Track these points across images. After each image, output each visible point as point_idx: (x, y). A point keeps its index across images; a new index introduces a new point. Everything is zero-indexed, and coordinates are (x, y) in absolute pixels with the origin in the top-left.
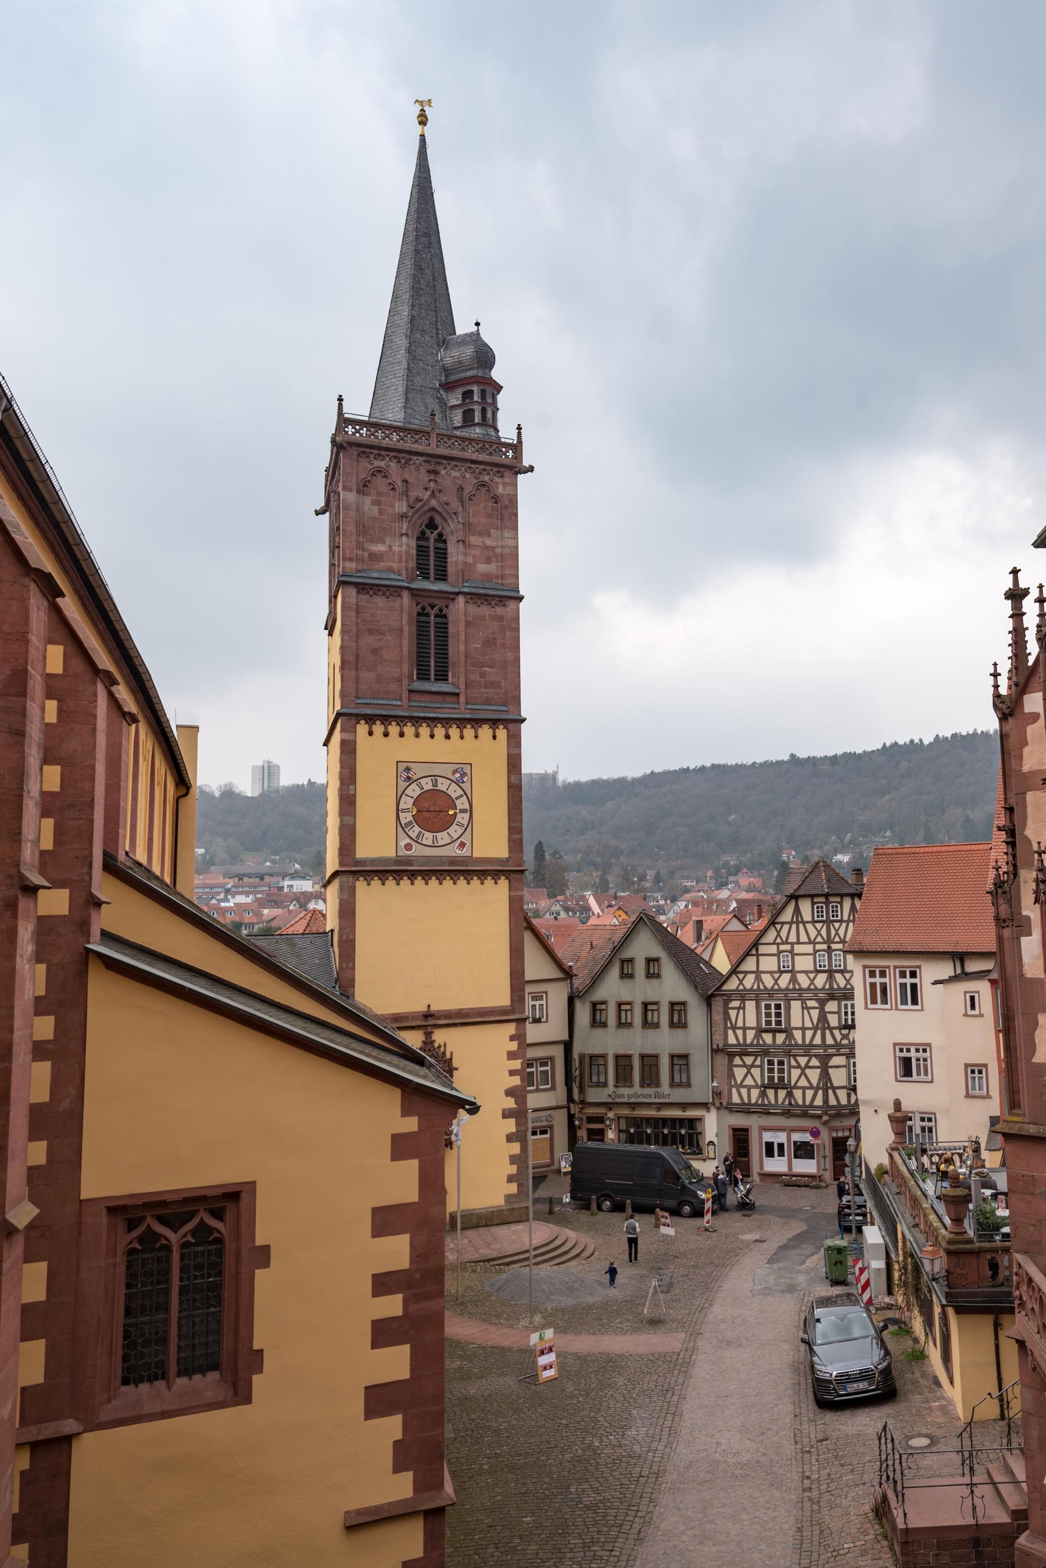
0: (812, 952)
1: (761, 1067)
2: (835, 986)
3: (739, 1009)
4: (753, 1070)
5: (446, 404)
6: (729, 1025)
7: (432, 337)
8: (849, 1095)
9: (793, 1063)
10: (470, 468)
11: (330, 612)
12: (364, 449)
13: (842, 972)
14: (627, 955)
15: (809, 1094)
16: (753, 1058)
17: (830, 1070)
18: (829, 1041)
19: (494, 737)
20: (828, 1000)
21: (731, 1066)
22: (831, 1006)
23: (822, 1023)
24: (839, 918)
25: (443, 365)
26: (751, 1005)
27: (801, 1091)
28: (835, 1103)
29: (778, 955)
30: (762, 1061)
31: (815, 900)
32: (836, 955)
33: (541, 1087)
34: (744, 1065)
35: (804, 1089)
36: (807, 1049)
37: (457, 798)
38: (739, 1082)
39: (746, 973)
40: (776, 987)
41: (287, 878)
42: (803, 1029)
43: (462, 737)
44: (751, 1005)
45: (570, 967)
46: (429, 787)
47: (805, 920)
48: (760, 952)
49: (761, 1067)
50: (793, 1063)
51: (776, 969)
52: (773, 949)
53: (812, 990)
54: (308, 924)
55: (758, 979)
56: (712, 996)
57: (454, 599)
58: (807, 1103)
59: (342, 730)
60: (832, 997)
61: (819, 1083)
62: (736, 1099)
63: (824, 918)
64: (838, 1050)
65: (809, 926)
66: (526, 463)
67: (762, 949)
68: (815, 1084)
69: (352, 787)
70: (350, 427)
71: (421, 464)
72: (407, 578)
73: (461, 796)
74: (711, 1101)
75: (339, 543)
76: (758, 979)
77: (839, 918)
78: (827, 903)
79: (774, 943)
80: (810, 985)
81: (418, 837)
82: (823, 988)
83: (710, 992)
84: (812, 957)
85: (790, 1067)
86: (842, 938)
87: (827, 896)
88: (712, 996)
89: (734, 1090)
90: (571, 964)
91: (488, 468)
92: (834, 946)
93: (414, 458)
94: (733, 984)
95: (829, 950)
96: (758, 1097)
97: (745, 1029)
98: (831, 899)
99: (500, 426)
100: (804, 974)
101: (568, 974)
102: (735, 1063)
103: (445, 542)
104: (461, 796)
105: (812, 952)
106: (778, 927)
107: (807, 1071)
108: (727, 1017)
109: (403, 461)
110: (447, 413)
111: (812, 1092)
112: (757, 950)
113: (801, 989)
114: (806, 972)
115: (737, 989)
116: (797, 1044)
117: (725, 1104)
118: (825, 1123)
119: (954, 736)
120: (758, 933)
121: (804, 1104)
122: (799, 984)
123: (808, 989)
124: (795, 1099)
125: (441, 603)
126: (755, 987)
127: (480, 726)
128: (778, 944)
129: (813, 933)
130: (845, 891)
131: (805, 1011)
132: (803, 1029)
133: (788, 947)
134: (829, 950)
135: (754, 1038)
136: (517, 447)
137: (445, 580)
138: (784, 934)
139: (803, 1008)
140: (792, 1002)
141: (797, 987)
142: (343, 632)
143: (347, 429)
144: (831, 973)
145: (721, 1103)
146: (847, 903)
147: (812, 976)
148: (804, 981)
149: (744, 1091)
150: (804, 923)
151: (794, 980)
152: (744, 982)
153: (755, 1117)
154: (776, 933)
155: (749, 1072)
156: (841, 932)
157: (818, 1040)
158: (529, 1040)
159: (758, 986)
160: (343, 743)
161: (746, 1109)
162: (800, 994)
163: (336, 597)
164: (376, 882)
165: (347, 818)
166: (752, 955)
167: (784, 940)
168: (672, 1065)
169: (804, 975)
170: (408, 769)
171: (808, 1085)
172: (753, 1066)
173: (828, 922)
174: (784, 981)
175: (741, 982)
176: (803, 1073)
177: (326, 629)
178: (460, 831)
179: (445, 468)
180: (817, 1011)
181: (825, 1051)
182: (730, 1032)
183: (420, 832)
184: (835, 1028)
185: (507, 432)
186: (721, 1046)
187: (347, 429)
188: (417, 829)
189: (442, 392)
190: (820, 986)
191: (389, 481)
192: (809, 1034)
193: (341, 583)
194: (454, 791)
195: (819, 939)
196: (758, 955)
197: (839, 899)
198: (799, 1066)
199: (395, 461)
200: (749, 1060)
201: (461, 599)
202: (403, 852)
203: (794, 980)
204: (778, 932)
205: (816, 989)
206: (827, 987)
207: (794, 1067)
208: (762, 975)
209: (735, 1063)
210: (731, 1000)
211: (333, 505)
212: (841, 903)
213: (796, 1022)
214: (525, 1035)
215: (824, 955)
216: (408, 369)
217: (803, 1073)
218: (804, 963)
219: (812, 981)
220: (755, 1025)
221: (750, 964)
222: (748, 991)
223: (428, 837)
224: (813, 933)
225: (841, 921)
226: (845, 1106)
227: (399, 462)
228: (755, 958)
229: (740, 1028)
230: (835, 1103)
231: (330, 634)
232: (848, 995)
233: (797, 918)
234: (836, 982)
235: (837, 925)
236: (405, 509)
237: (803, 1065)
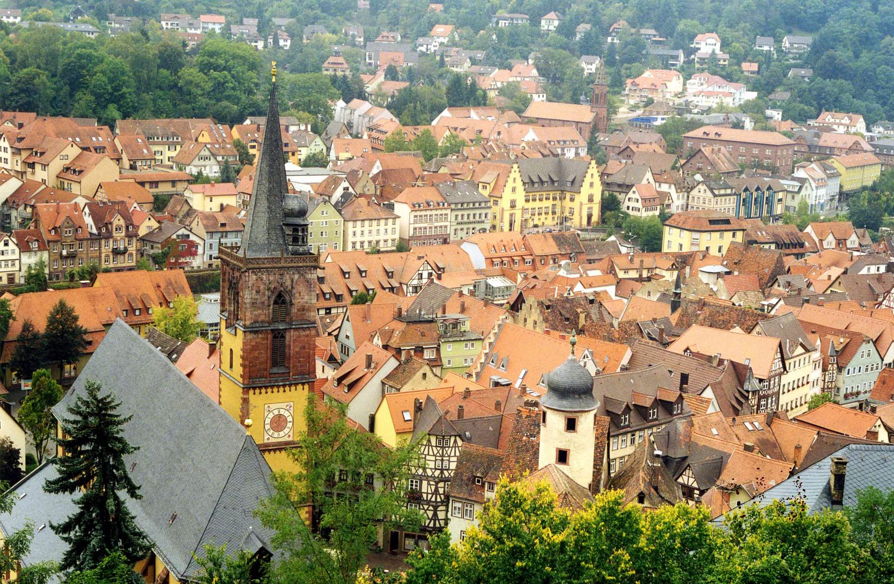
13: (447, 470)
18: (439, 500)
22: (441, 484)
36: (428, 502)
42: (427, 493)
50: (421, 507)
60: (441, 481)
65: (434, 448)
68: (430, 517)
92: (444, 458)
95: (442, 460)
123: (431, 476)
125: (282, 332)
129: (436, 451)
132: (427, 493)
134: (442, 460)
144: (442, 470)
148: (429, 473)
150: (432, 446)
156: (449, 452)
157: (433, 499)
162: (427, 478)
173: (443, 448)
178: (288, 430)
188: (272, 431)
189: (284, 227)
190: (436, 476)
192: (430, 496)
194: (286, 414)
198: (424, 509)
202: (266, 441)
213: (424, 490)
218: (431, 465)
219: (433, 473)
223: (276, 435)
224: (436, 451)
225: (449, 447)
235: (447, 449)
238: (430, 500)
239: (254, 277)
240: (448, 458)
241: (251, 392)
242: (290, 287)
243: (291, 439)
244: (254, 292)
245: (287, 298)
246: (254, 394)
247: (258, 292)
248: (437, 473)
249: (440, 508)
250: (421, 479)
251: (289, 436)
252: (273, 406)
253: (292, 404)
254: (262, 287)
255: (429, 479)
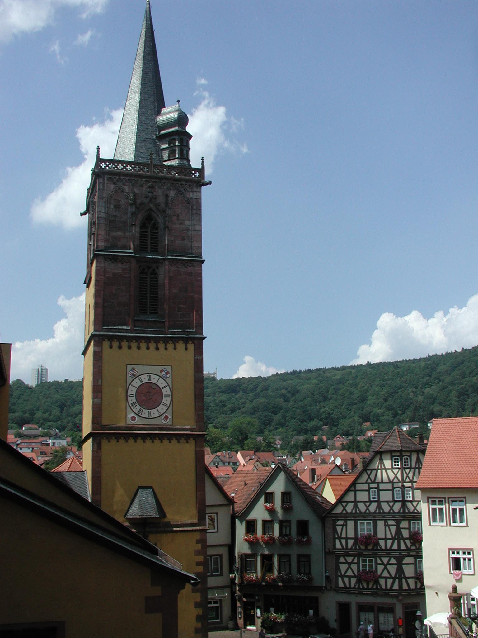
0: (391, 488)
1: (358, 563)
2: (407, 511)
3: (342, 526)
4: (352, 566)
6: (336, 536)
8: (416, 583)
9: (379, 561)
11: (88, 273)
12: (110, 173)
14: (270, 490)
15: (390, 581)
16: (352, 558)
17: (404, 566)
18: (403, 547)
19: (186, 349)
20: (402, 520)
21: (338, 563)
23: (398, 535)
24: (409, 466)
26: (351, 524)
27: (384, 580)
28: (407, 588)
29: (368, 491)
30: (358, 560)
31: (394, 454)
32: (407, 490)
33: (214, 574)
34: (346, 562)
35: (386, 578)
36: (388, 552)
37: (163, 388)
38: (343, 574)
39: (348, 502)
40: (368, 511)
41: (52, 438)
42: (386, 539)
43: (166, 349)
44: (351, 524)
45: (233, 497)
46: (146, 380)
47: (386, 467)
48: (357, 489)
49: (358, 563)
50: (379, 561)
51: (367, 500)
52: (365, 487)
53: (391, 513)
54: (70, 466)
55: (356, 506)
56: (325, 517)
57: (162, 263)
58: (388, 588)
59: (95, 345)
60: (404, 518)
61: (396, 575)
62: (341, 584)
63: (399, 466)
64: (409, 553)
66: (207, 180)
67: (358, 487)
68: (393, 576)
69: (100, 381)
70: (103, 163)
72: (134, 249)
73: (166, 386)
74: (324, 585)
75: (94, 232)
76: (356, 506)
77: (409, 466)
78: (401, 456)
79: (366, 483)
80: (390, 511)
81: (139, 412)
82: (399, 513)
83: (324, 515)
84: (391, 492)
85: (377, 564)
86: (411, 479)
87: (401, 451)
88: (325, 517)
89: (340, 579)
90: (233, 495)
94: (339, 510)
96: (356, 584)
97: (347, 539)
98: (404, 454)
99: (191, 157)
100: (386, 503)
101: (231, 502)
102: (340, 561)
103: (157, 228)
104: (166, 386)
105: (391, 488)
106: (369, 472)
107: (388, 567)
108: (335, 531)
109: (133, 182)
111: (392, 580)
112: (355, 487)
113: (384, 513)
114: (388, 502)
115: (342, 513)
116: (381, 549)
117: (333, 587)
118: (400, 601)
119: (446, 353)
120: (355, 477)
121: (386, 589)
122: (383, 510)
123: (389, 513)
124: (380, 585)
126: (354, 512)
127: (178, 342)
128: (369, 484)
130: (413, 448)
131: (387, 527)
132: (386, 539)
133: (375, 485)
135: (353, 545)
136: (201, 171)
137: (157, 251)
138: (372, 477)
139: (385, 526)
140: (378, 522)
141: (382, 512)
142: (96, 285)
143: (101, 165)
145: (331, 587)
146: (414, 457)
147: (391, 504)
149: (346, 580)
151: (379, 507)
152: (346, 508)
153: (353, 596)
154: (367, 476)
155: (349, 567)
157: (395, 547)
158: (209, 543)
159: (356, 511)
160: (95, 354)
161: (347, 590)
162: (383, 516)
163: (92, 264)
164: (113, 441)
165: (96, 400)
166: (352, 491)
167: (373, 480)
168: (299, 562)
169: (386, 503)
170: (133, 369)
171: (389, 576)
172: (352, 563)
174: (373, 507)
175: (344, 508)
176: (385, 568)
177: (85, 283)
178: (165, 408)
180: (395, 527)
181: (400, 553)
182: (337, 541)
183: (140, 409)
184: (407, 539)
185: (195, 163)
186: (331, 550)
187: (101, 165)
188: (138, 407)
190: (396, 511)
192: (389, 542)
193: (95, 256)
194: (161, 383)
195: (396, 480)
196: (355, 491)
197: (408, 454)
198: (382, 563)
200: (349, 559)
201: (167, 263)
203: (379, 507)
204: (369, 475)
205: (394, 513)
206: (401, 511)
207: (380, 564)
208: (358, 504)
209: (340, 561)
210: (338, 520)
211: (91, 209)
212: (410, 456)
213: (381, 534)
214: (206, 539)
215: (399, 490)
217: (385, 568)
219: (391, 508)
220: (354, 537)
221: (350, 497)
222: (349, 514)
223: (145, 413)
225: (410, 468)
226: (413, 590)
228: (353, 492)
229: (343, 538)
230: (407, 588)
231: (88, 286)
232: (417, 517)
233: (381, 467)
234: (408, 508)
235: (407, 471)
236: (134, 210)
237: (385, 563)
238: (391, 549)
239: (112, 187)
240: (410, 485)
241: (106, 344)
242: (163, 206)
243: (169, 422)
244: (112, 206)
245: (160, 220)
246: (111, 347)
247: (117, 207)
248: (397, 507)
249: (407, 560)
250: (374, 518)
251: (166, 417)
252: (139, 369)
253: (169, 369)
254: (123, 202)
255: (387, 517)
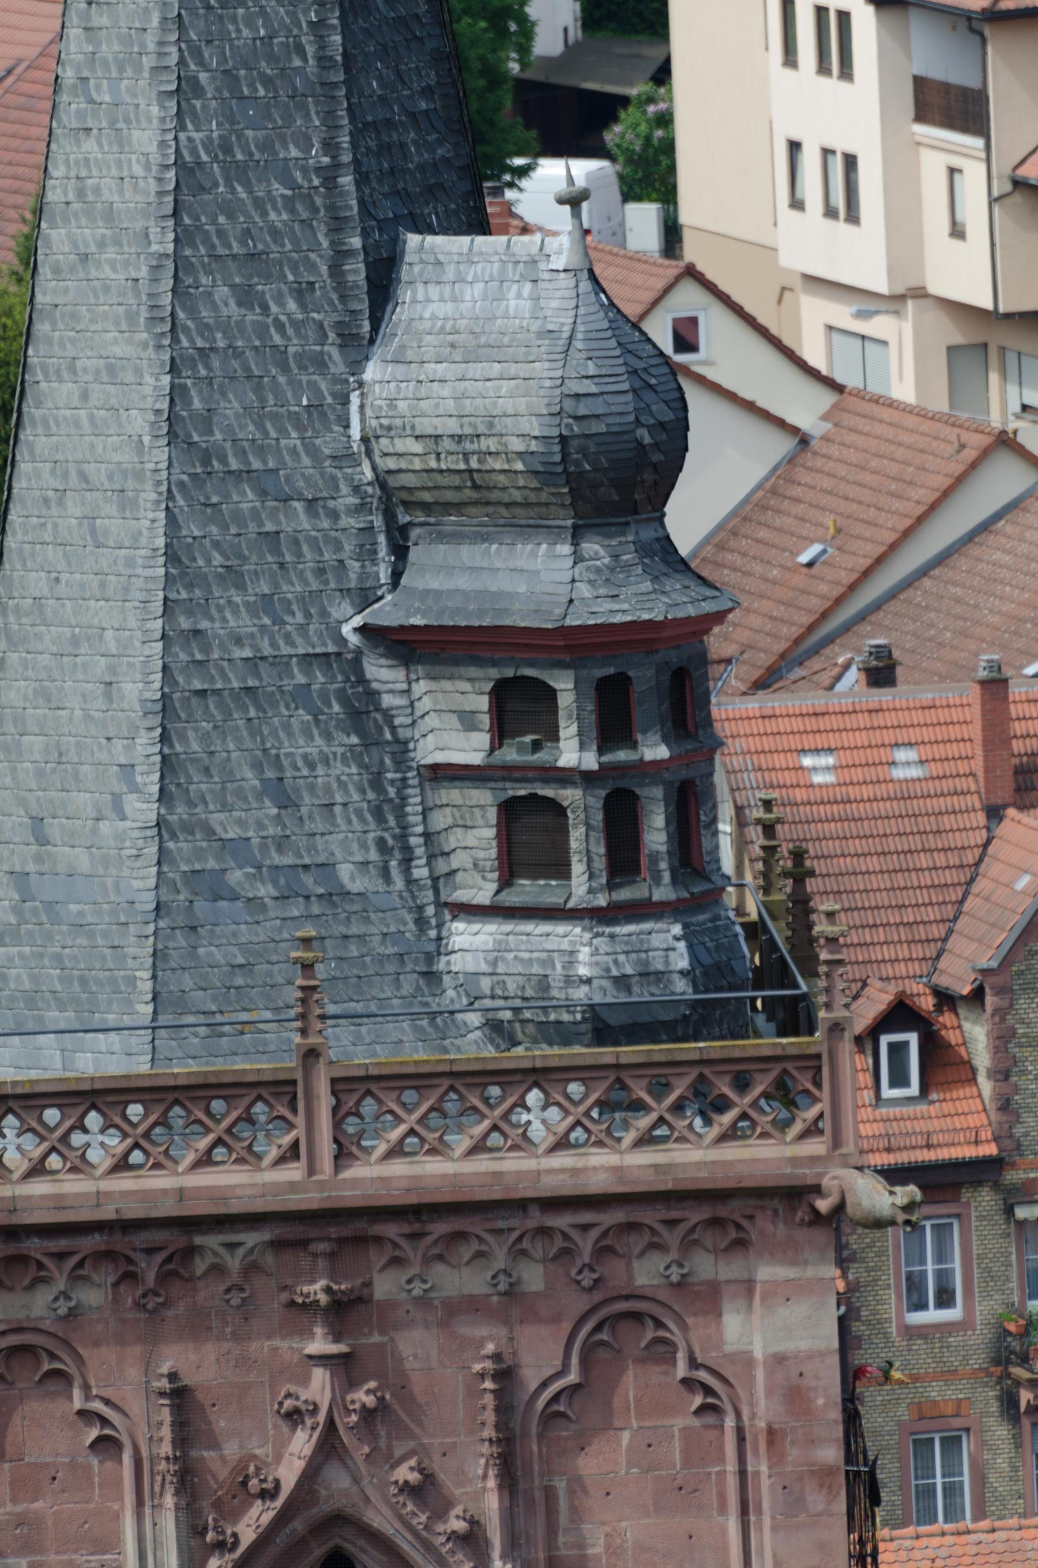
5: (402, 749)
7: (303, 292)
10: (544, 1232)
25: (381, 480)
71: (251, 1269)
91: (649, 1216)
93: (212, 1241)
110: (414, 807)
179: (397, 1262)
191: (78, 1401)
199: (108, 1275)
216: (171, 556)
227: (130, 1277)
